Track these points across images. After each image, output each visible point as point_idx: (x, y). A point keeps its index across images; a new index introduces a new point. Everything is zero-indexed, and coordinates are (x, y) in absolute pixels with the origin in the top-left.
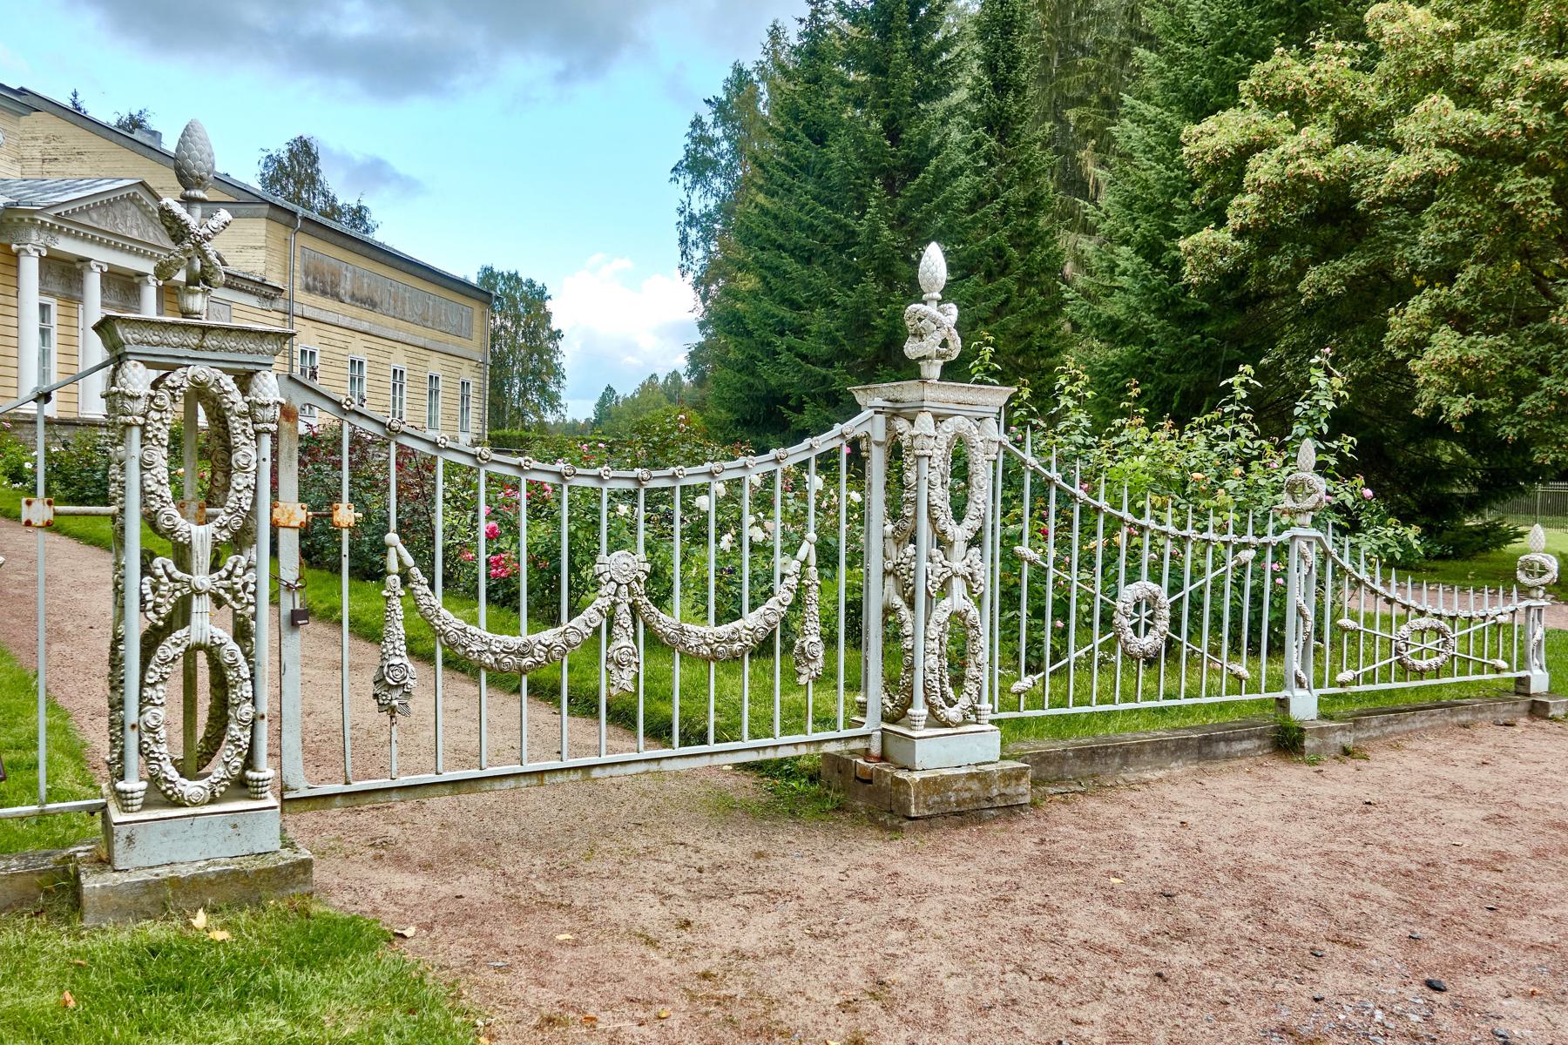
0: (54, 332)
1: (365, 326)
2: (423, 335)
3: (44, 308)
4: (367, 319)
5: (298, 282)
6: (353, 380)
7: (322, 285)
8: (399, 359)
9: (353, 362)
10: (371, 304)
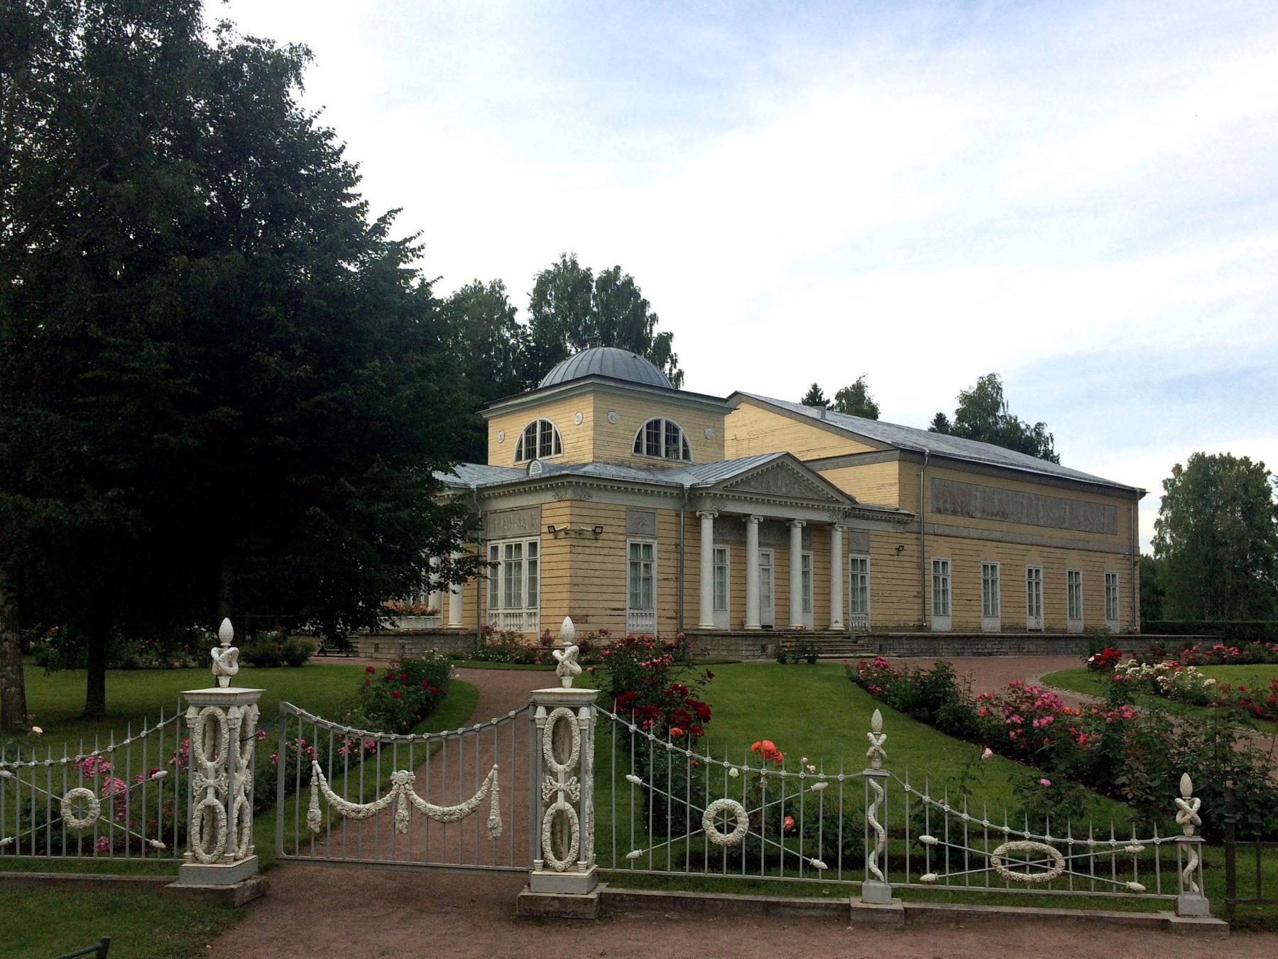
1: (997, 535)
2: (1058, 536)
4: (997, 528)
5: (928, 508)
6: (985, 581)
7: (952, 505)
8: (1034, 560)
9: (985, 567)
10: (1004, 516)
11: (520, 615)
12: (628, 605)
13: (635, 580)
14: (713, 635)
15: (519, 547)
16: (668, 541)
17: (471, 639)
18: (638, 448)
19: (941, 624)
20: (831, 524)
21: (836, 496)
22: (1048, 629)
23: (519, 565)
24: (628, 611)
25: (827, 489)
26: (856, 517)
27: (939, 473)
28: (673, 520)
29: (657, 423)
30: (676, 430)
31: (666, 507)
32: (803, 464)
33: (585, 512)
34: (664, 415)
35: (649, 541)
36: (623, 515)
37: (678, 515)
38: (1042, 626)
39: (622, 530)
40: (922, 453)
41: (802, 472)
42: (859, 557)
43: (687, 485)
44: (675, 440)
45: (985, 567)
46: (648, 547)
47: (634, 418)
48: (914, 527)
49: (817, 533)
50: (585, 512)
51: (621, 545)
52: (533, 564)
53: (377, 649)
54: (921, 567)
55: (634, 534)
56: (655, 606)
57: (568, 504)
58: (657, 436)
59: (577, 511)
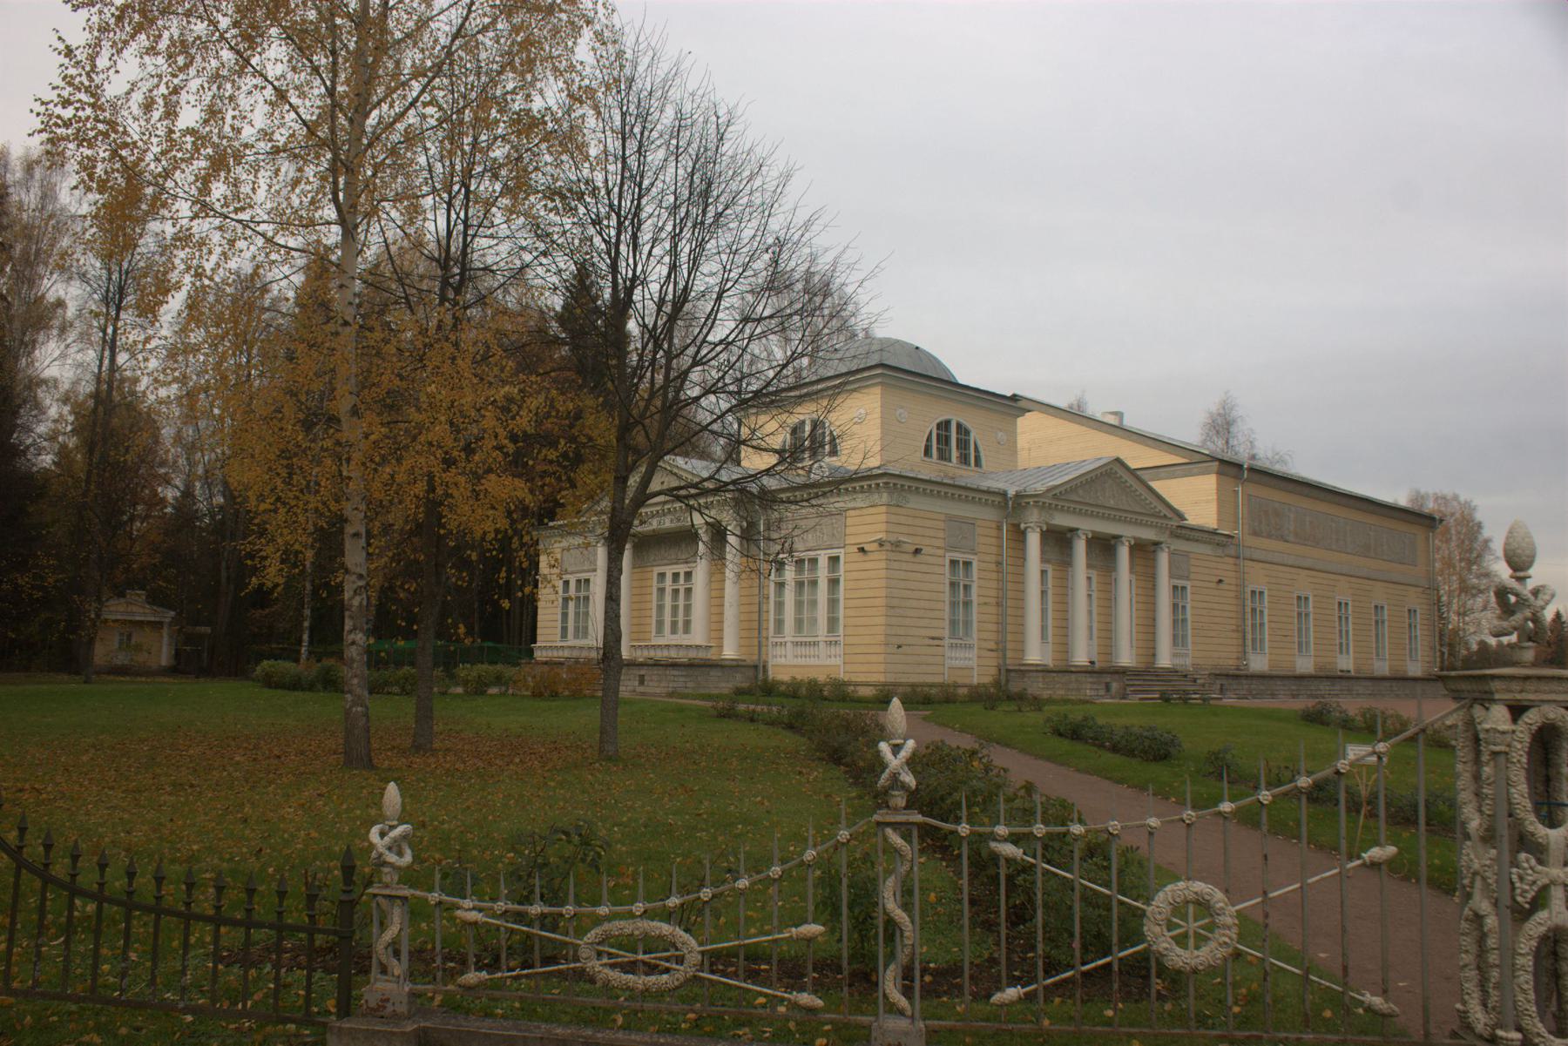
0: (1050, 593)
3: (1043, 572)
6: (1299, 614)
9: (1299, 598)
11: (815, 644)
12: (946, 633)
13: (953, 605)
14: (1044, 670)
15: (814, 561)
16: (988, 558)
17: (751, 673)
18: (927, 452)
19: (1258, 663)
20: (1157, 544)
21: (1165, 511)
22: (1357, 671)
23: (814, 583)
24: (947, 642)
25: (1156, 503)
26: (1178, 537)
27: (1253, 489)
28: (994, 533)
29: (947, 423)
30: (967, 432)
31: (986, 516)
32: (1133, 472)
33: (903, 520)
34: (956, 414)
35: (968, 557)
36: (941, 525)
37: (999, 528)
38: (1351, 667)
39: (939, 543)
40: (1239, 466)
41: (1131, 481)
42: (1180, 583)
43: (1011, 492)
44: (967, 443)
45: (1299, 598)
46: (967, 564)
47: (926, 415)
48: (1232, 551)
49: (1144, 552)
50: (903, 520)
51: (939, 561)
52: (834, 583)
53: (642, 682)
54: (1239, 596)
55: (953, 548)
56: (975, 635)
57: (884, 509)
58: (947, 440)
59: (894, 518)
